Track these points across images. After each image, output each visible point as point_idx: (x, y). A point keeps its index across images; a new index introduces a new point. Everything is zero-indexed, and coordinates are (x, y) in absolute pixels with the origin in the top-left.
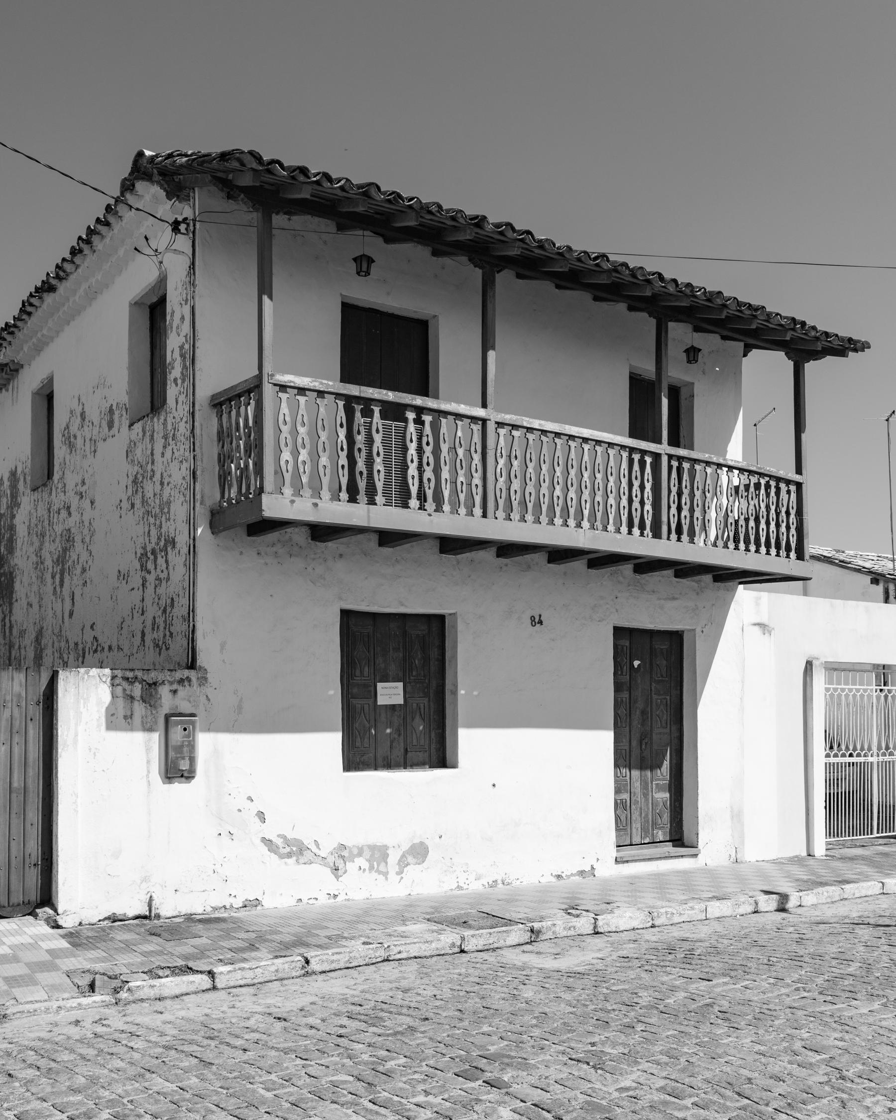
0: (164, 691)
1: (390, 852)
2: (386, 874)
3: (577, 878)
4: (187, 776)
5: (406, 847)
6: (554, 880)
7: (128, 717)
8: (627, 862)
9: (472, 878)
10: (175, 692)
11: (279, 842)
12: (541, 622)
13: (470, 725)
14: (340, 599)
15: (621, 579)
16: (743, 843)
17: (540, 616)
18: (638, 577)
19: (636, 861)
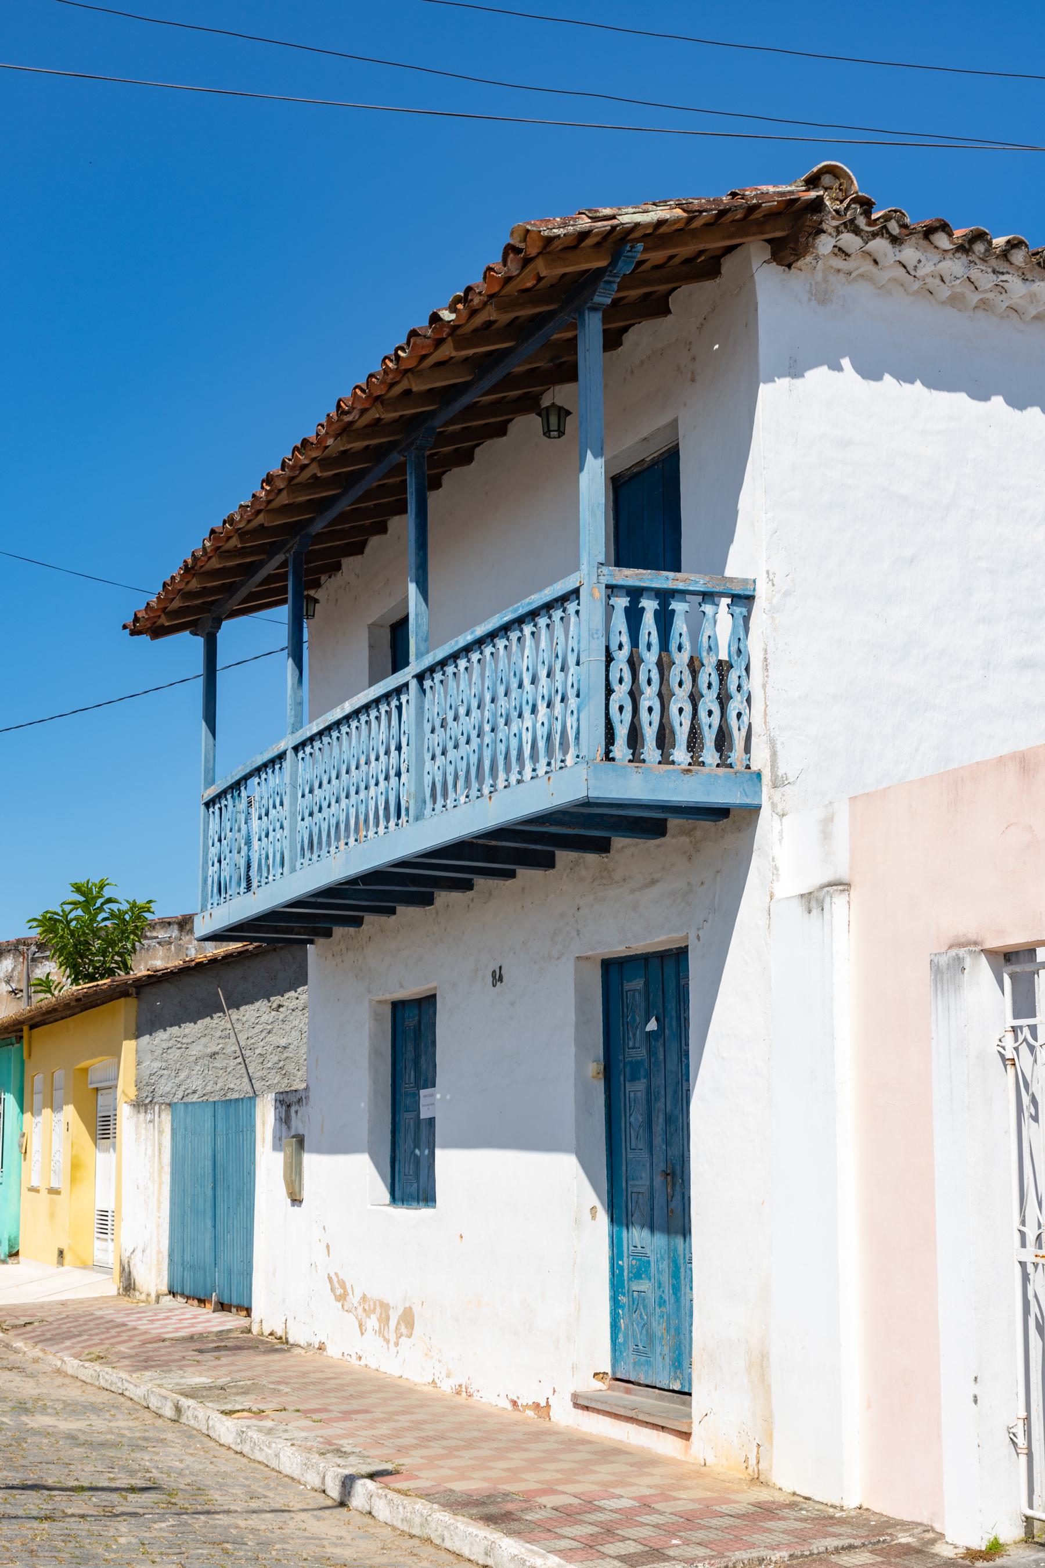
0: (293, 1109)
1: (391, 1313)
2: (388, 1341)
3: (530, 1413)
4: (301, 1202)
5: (400, 1311)
6: (509, 1406)
7: (280, 1139)
8: (587, 1408)
9: (444, 1375)
10: (296, 1112)
11: (335, 1279)
12: (501, 979)
13: (444, 1146)
14: (369, 991)
15: (583, 872)
16: (770, 1435)
17: (500, 968)
18: (475, 887)
19: (598, 1411)
